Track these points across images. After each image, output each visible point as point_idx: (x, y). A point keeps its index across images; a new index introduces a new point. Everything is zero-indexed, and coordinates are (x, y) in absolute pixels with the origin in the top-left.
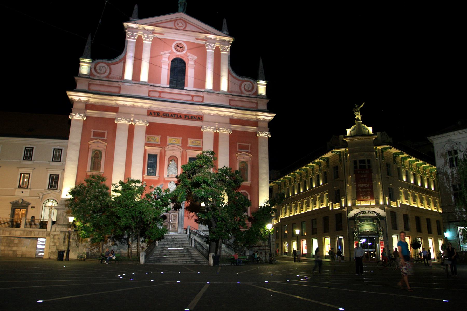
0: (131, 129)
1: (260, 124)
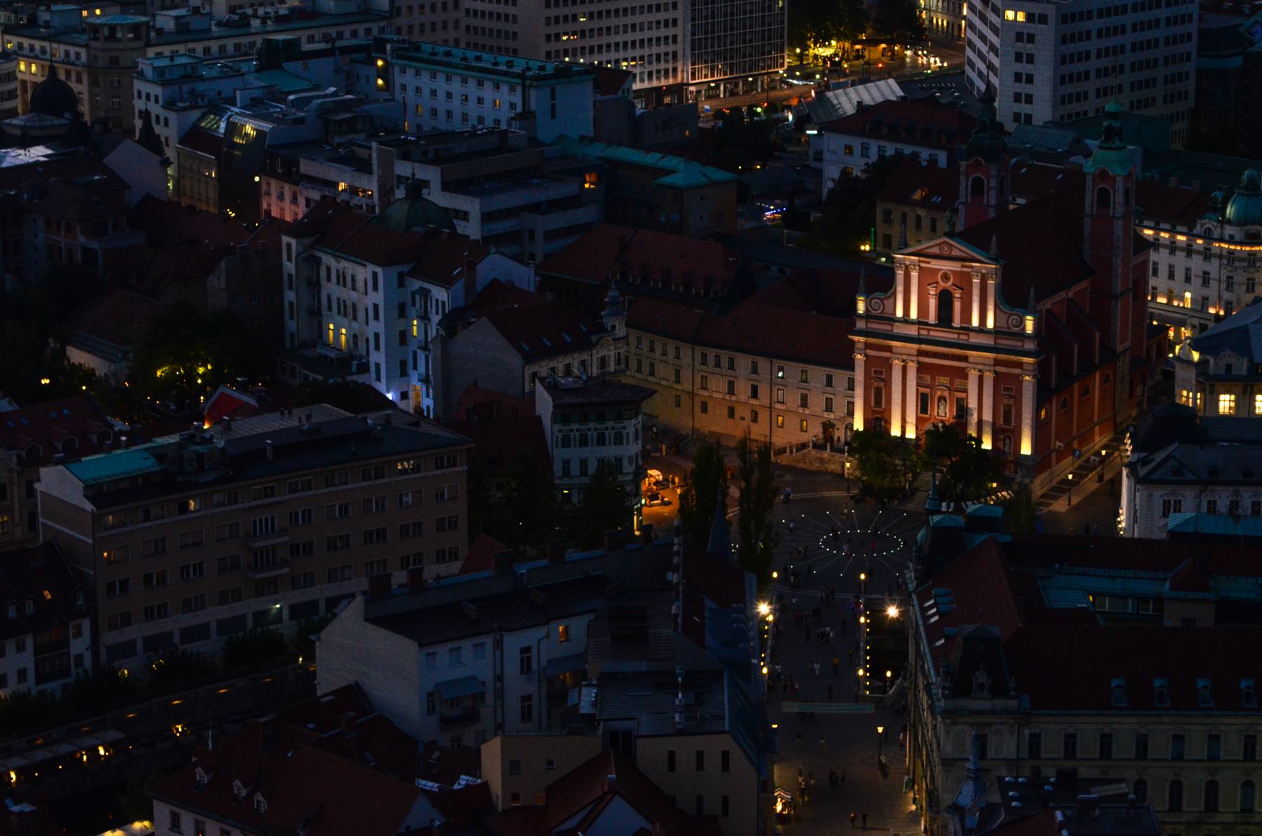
0: (904, 369)
1: (1025, 367)
